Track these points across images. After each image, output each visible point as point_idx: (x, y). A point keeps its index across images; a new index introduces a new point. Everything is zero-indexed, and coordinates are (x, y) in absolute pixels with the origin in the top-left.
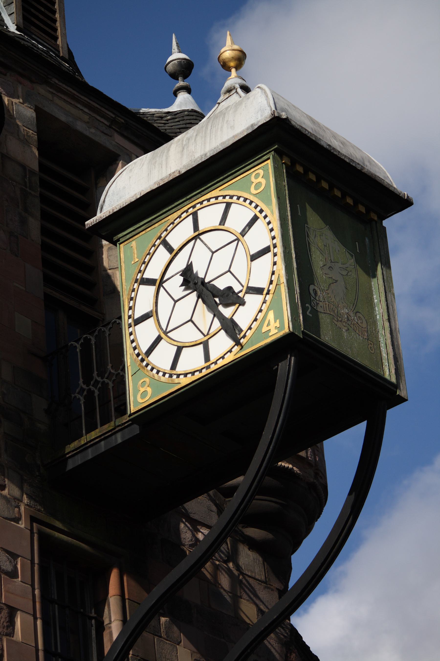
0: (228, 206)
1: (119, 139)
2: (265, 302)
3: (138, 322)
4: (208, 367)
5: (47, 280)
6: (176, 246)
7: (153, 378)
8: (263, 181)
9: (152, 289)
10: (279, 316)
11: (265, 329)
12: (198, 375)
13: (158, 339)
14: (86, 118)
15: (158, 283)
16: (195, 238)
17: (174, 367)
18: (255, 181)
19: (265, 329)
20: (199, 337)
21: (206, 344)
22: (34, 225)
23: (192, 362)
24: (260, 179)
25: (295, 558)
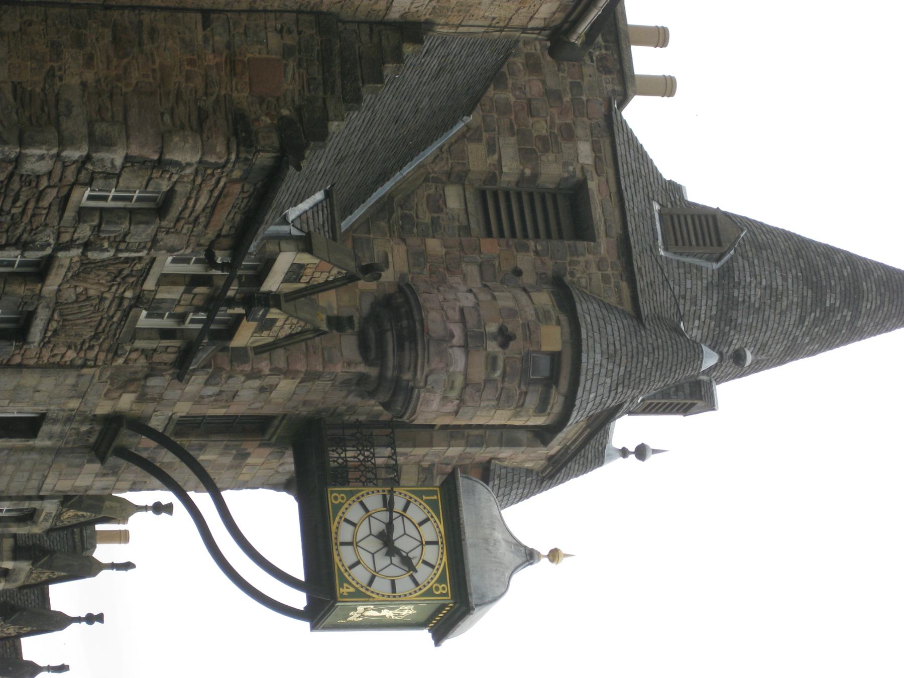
0: (433, 567)
1: (557, 448)
2: (362, 587)
4: (336, 544)
6: (421, 529)
7: (343, 504)
8: (437, 593)
10: (350, 595)
11: (345, 585)
12: (334, 535)
13: (367, 510)
14: (569, 437)
16: (422, 542)
17: (346, 521)
18: (440, 587)
19: (345, 585)
21: (350, 544)
23: (345, 533)
24: (441, 591)
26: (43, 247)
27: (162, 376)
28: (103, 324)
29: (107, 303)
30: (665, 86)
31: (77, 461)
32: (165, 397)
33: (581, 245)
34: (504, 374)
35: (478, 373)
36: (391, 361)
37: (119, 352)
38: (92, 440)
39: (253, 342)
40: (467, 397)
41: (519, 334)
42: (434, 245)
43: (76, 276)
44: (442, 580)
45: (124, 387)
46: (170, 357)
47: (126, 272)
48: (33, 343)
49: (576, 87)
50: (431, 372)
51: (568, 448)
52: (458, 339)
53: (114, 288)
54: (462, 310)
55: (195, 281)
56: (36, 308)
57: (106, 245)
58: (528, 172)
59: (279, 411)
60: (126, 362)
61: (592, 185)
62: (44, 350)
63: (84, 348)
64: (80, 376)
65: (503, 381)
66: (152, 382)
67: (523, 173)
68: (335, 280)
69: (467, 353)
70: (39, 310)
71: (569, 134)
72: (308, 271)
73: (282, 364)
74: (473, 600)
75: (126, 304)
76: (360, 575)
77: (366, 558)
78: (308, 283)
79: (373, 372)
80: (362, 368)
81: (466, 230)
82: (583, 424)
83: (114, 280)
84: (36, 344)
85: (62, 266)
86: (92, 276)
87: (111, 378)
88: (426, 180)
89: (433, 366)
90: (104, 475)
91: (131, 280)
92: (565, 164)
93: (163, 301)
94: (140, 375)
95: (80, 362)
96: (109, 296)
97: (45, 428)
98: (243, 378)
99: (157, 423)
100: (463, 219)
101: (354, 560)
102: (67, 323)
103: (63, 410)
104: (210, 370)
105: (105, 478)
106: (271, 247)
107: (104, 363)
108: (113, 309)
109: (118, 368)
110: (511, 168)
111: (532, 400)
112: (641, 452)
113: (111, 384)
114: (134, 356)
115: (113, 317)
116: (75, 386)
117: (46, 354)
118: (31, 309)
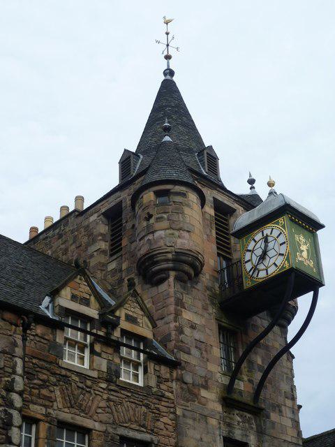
0: (273, 229)
3: (246, 262)
5: (218, 248)
9: (250, 253)
10: (289, 262)
15: (252, 251)
20: (265, 267)
22: (214, 232)
23: (262, 274)
25: (289, 327)
26: (11, 416)
27: (182, 374)
28: (132, 400)
29: (111, 397)
30: (80, 199)
31: (268, 424)
32: (203, 374)
33: (124, 205)
34: (165, 213)
35: (165, 224)
36: (164, 266)
37: (160, 394)
38: (248, 415)
39: (148, 326)
40: (178, 227)
41: (146, 211)
42: (124, 266)
43: (83, 411)
44: (277, 223)
45: (196, 396)
46: (164, 371)
47: (81, 385)
48: (152, 439)
49: (72, 232)
50: (165, 245)
51: (235, 200)
52: (150, 237)
53: (97, 392)
54: (140, 240)
55: (93, 352)
56: (118, 435)
57: (6, 379)
58: (100, 238)
59: (213, 321)
60: (172, 392)
61: (103, 210)
62: (160, 433)
63: (158, 412)
64: (184, 416)
65: (167, 213)
66: (188, 378)
67: (100, 240)
68: (86, 281)
69: (156, 231)
70: (119, 433)
71: (88, 226)
72: (76, 293)
73: (172, 317)
74: (282, 204)
75: (113, 388)
76: (280, 260)
77: (272, 261)
78: (90, 295)
79: (172, 274)
80: (171, 279)
81: (121, 256)
82: (215, 192)
83: (90, 392)
84: (154, 437)
85: (72, 418)
86: (84, 403)
87: (188, 401)
88: (105, 280)
89: (163, 244)
90: (280, 411)
91: (89, 383)
92: (97, 224)
93: (109, 368)
94: (185, 386)
95: (172, 416)
96: (105, 396)
97: (238, 435)
98: (182, 336)
99: (225, 380)
100: (118, 259)
101: (273, 266)
102: (133, 419)
103: (220, 428)
104: (175, 350)
105: (284, 412)
106: (57, 310)
107: (173, 403)
108: (119, 395)
109: (177, 397)
110: (103, 245)
111: (178, 199)
112: (251, 182)
113: (194, 401)
114: (163, 387)
115: (128, 396)
116: (194, 419)
117: (164, 432)
118: (118, 438)
